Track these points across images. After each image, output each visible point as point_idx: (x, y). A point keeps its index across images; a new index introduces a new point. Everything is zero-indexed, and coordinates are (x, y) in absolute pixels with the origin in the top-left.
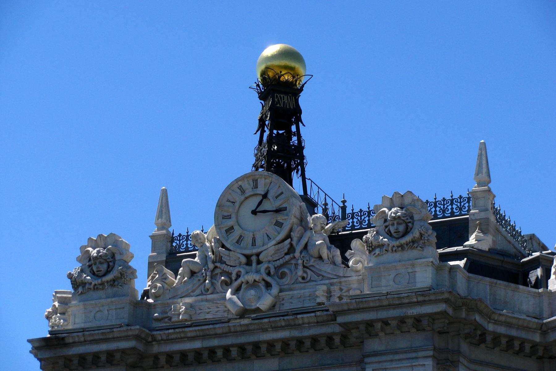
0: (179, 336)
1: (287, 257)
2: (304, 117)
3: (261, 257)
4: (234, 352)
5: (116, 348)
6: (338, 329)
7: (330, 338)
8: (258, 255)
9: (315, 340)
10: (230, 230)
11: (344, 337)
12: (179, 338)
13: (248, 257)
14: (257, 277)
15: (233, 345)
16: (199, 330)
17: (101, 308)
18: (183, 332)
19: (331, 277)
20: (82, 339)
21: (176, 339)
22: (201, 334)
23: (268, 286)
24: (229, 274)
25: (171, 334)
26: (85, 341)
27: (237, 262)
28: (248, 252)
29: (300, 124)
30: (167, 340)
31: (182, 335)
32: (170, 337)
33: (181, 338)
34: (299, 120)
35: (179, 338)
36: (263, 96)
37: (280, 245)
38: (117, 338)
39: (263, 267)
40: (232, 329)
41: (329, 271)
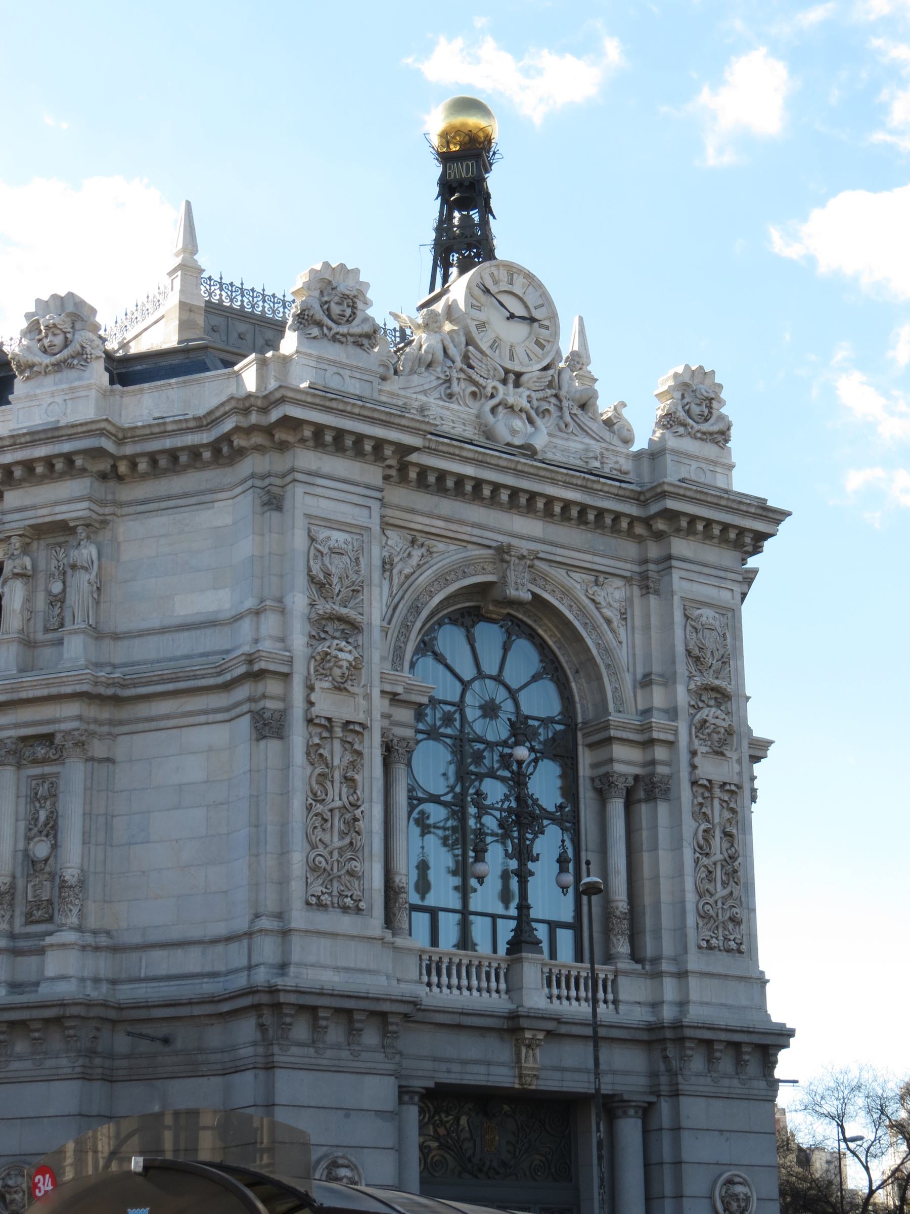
0: (451, 450)
1: (549, 392)
3: (524, 379)
4: (504, 496)
5: (396, 440)
8: (518, 375)
9: (601, 513)
10: (482, 326)
12: (450, 454)
13: (507, 372)
15: (506, 487)
16: (480, 453)
17: (341, 371)
18: (461, 448)
19: (598, 438)
20: (357, 411)
21: (447, 453)
22: (480, 458)
25: (443, 443)
26: (359, 415)
27: (491, 373)
28: (509, 365)
29: (491, 217)
30: (435, 450)
31: (457, 452)
32: (441, 448)
33: (454, 454)
35: (450, 454)
37: (543, 373)
38: (404, 426)
39: (524, 392)
40: (519, 467)
41: (594, 428)
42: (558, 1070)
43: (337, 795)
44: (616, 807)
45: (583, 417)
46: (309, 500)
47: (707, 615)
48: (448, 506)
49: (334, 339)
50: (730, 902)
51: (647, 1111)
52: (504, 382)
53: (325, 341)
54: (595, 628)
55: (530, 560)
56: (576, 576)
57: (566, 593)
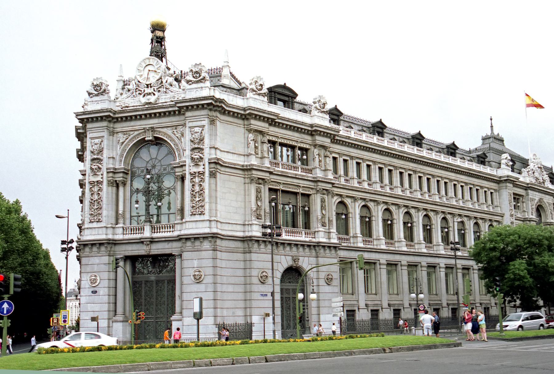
2: (166, 39)
6: (177, 109)
7: (174, 111)
8: (150, 84)
11: (179, 111)
13: (147, 85)
14: (150, 92)
23: (154, 94)
24: (141, 91)
28: (148, 83)
34: (164, 40)
36: (152, 32)
42: (157, 249)
43: (96, 197)
44: (179, 183)
45: (171, 88)
46: (91, 134)
47: (197, 129)
48: (132, 123)
49: (97, 95)
50: (201, 201)
51: (181, 255)
52: (148, 87)
53: (95, 97)
54: (174, 141)
55: (153, 129)
56: (169, 129)
57: (165, 134)
